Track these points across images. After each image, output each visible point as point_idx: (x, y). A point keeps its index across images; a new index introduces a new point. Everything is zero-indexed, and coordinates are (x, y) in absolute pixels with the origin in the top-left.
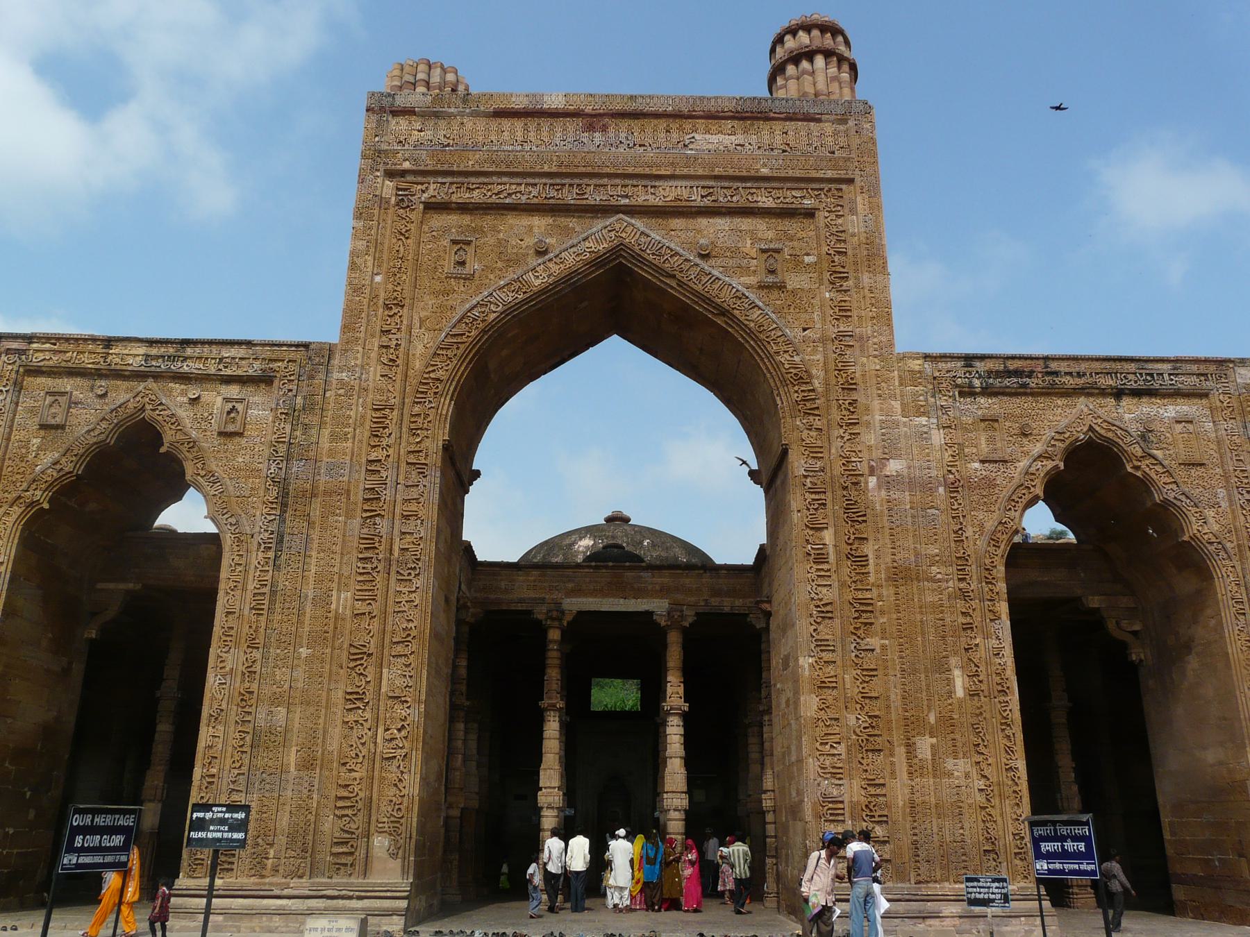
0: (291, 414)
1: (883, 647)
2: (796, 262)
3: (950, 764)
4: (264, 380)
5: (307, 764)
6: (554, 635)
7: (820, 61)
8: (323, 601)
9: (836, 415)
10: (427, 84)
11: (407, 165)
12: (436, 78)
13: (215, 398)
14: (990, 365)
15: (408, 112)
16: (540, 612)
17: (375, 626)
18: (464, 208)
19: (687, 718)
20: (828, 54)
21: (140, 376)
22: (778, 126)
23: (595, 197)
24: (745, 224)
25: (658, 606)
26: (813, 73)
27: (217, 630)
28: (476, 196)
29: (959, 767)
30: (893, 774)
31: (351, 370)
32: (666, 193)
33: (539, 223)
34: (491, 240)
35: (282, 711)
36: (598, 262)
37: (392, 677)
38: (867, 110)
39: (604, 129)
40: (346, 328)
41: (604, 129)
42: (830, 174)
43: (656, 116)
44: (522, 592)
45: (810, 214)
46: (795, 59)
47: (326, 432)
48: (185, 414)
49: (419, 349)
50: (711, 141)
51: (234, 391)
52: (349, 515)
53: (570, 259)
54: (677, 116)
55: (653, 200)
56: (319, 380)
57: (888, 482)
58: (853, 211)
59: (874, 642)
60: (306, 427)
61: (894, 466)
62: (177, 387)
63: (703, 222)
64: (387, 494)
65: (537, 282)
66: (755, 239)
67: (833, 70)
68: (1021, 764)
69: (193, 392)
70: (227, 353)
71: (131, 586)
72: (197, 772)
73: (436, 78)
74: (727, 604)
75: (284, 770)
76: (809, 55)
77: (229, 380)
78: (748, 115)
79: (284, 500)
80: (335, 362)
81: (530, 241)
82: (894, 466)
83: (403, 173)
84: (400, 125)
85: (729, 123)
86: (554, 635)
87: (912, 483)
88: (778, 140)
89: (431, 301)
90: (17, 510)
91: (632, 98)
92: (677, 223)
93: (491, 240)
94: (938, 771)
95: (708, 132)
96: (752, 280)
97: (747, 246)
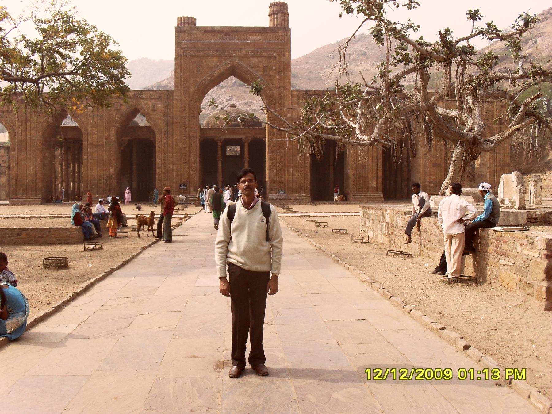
0: (167, 106)
1: (285, 152)
2: (271, 69)
3: (295, 173)
4: (160, 98)
5: (177, 175)
6: (220, 144)
7: (279, 15)
8: (177, 145)
9: (277, 104)
10: (188, 23)
11: (185, 46)
12: (190, 21)
13: (150, 103)
14: (311, 93)
15: (184, 31)
16: (216, 139)
17: (188, 149)
18: (199, 56)
19: (249, 162)
20: (281, 13)
21: (134, 98)
22: (269, 34)
23: (227, 54)
24: (260, 59)
25: (242, 137)
26: (277, 18)
27: (157, 151)
28: (201, 54)
29: (296, 174)
30: (285, 175)
31: (177, 96)
32: (243, 52)
33: (215, 60)
34: (205, 64)
35: (171, 166)
36: (228, 69)
37: (192, 159)
38: (290, 29)
39: (229, 35)
40: (175, 87)
41: (229, 35)
42: (280, 47)
43: (241, 31)
44: (211, 134)
45: (275, 57)
46: (274, 14)
47: (174, 110)
48: (144, 106)
49: (192, 90)
50: (253, 38)
51: (153, 101)
52: (180, 127)
53: (222, 69)
54: (245, 31)
55: (241, 54)
56: (171, 99)
57: (287, 119)
58: (284, 56)
59: (283, 151)
60: (170, 109)
61: (289, 116)
62: (141, 100)
63: (251, 59)
64: (187, 123)
65: (216, 74)
66: (263, 63)
67: (283, 17)
68: (308, 173)
69: (146, 102)
70: (151, 93)
71: (129, 138)
72: (157, 177)
73: (190, 21)
74: (258, 136)
75: (173, 176)
76: (277, 14)
77: (152, 99)
78: (262, 31)
79: (167, 125)
80: (175, 94)
81: (214, 64)
82: (289, 116)
83: (184, 48)
84: (183, 35)
85: (257, 34)
86: (220, 144)
87: (292, 119)
88: (269, 38)
89: (193, 79)
90: (114, 128)
91: (236, 27)
92: (246, 59)
93: (205, 64)
94: (293, 174)
95: (253, 36)
96: (261, 73)
97: (261, 65)
